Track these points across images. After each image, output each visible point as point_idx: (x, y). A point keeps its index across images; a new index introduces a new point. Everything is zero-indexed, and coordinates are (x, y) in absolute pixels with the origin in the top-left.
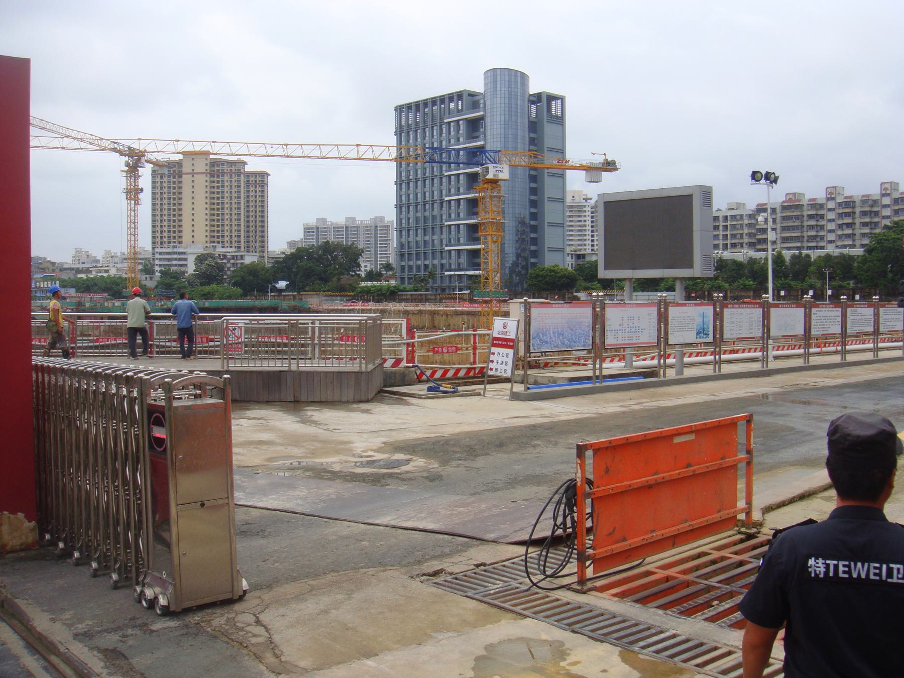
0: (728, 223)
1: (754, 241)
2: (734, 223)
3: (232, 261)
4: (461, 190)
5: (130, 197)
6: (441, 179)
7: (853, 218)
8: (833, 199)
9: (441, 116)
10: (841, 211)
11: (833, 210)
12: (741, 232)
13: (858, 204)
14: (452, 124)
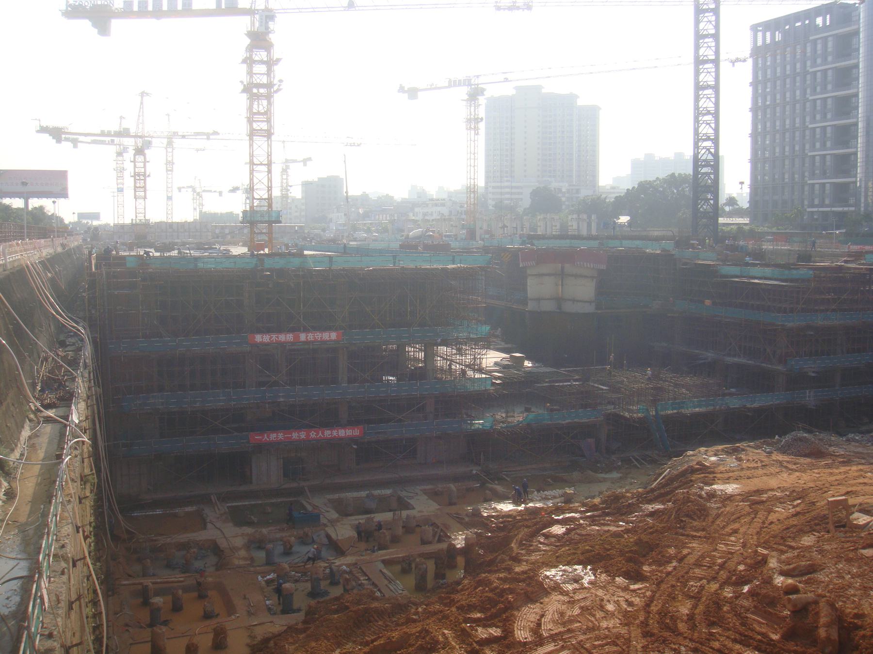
3: (567, 195)
5: (470, 127)
14: (819, 41)
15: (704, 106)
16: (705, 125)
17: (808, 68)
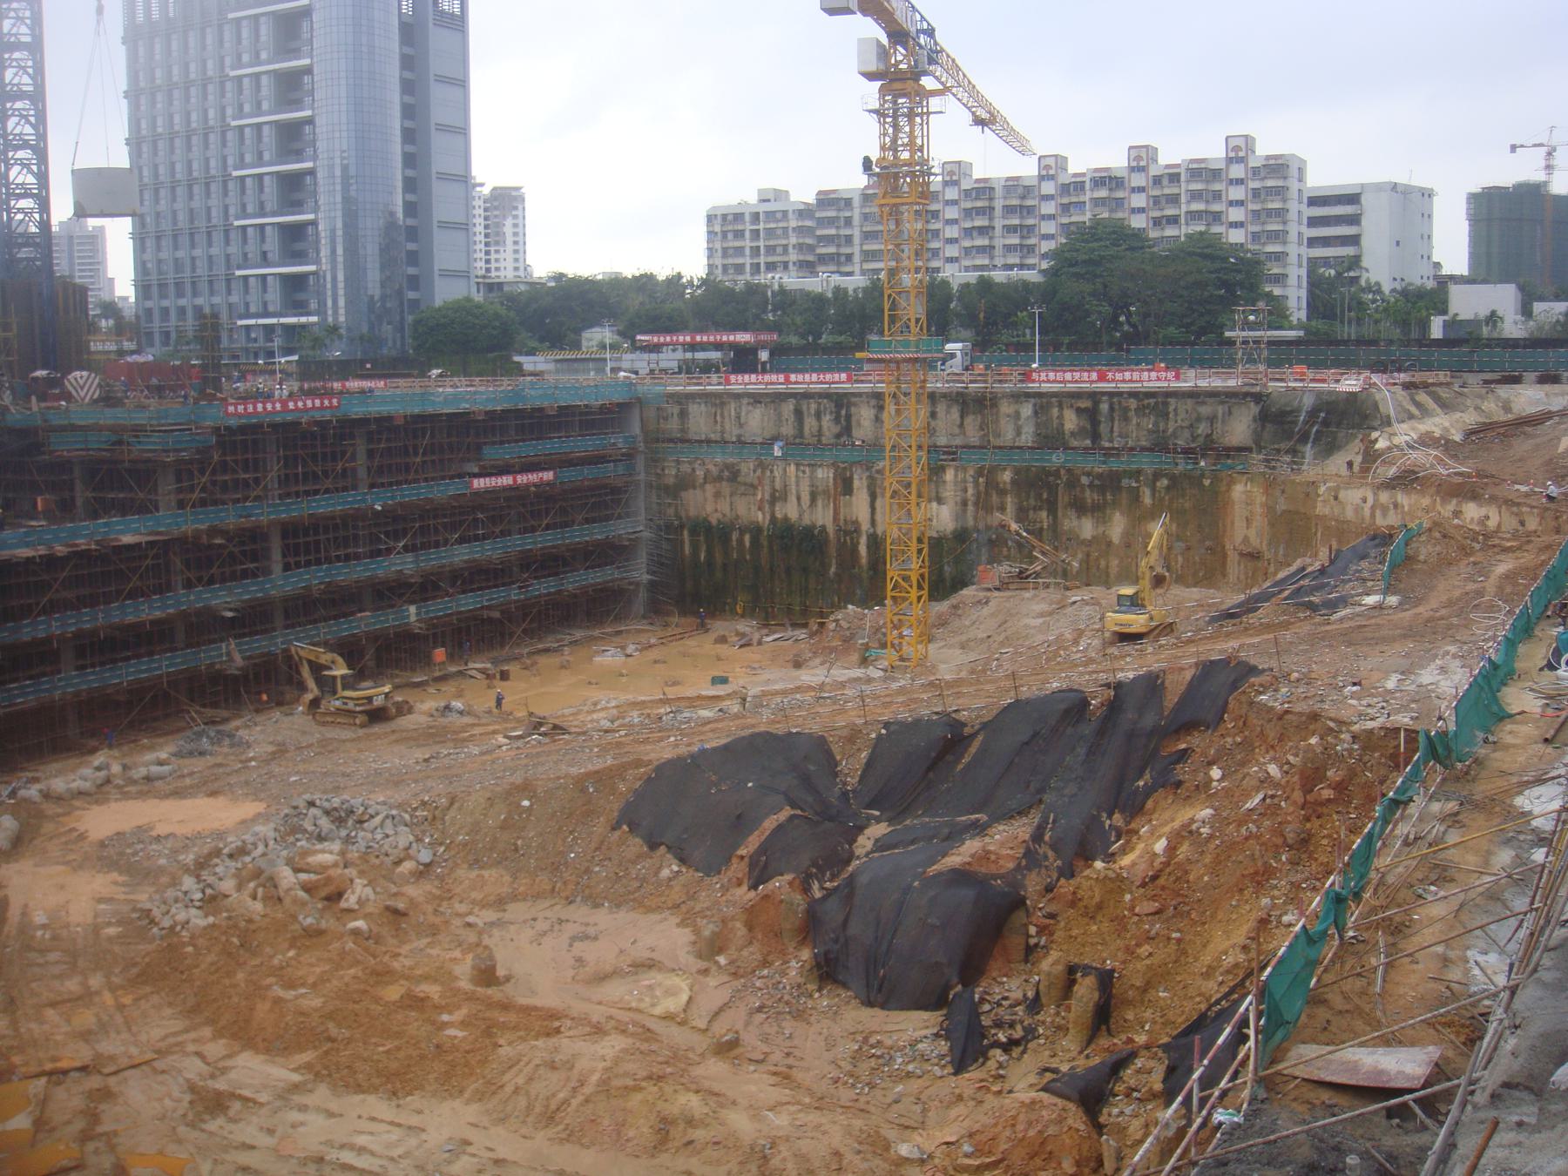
0: (761, 226)
1: (811, 258)
2: (772, 225)
4: (267, 156)
6: (224, 133)
7: (991, 219)
8: (956, 183)
10: (969, 205)
11: (954, 202)
12: (784, 242)
13: (999, 193)
14: (244, 23)
15: (17, 131)
16: (19, 168)
17: (227, 70)
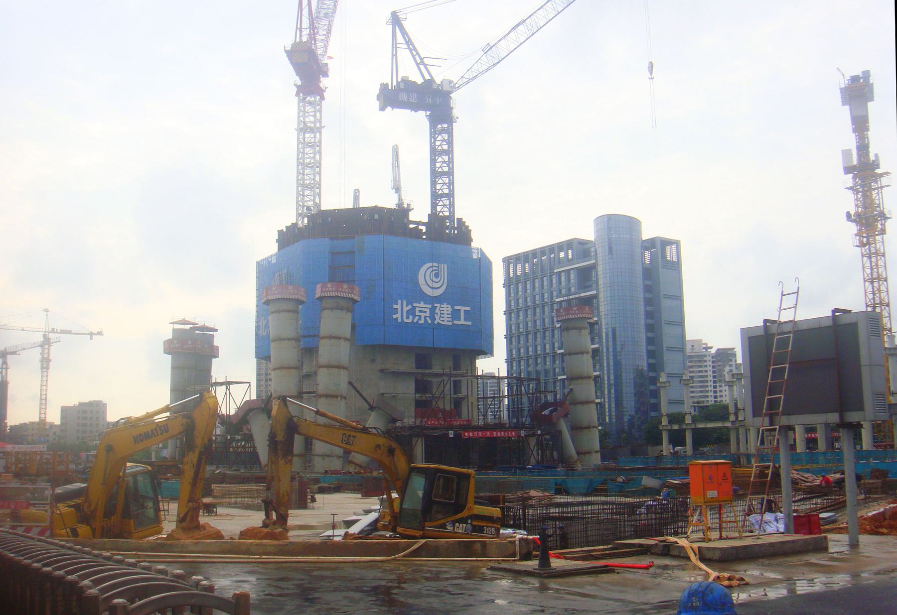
9: (550, 264)
14: (563, 274)
